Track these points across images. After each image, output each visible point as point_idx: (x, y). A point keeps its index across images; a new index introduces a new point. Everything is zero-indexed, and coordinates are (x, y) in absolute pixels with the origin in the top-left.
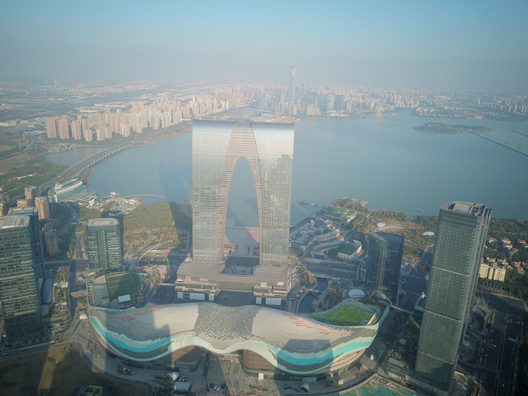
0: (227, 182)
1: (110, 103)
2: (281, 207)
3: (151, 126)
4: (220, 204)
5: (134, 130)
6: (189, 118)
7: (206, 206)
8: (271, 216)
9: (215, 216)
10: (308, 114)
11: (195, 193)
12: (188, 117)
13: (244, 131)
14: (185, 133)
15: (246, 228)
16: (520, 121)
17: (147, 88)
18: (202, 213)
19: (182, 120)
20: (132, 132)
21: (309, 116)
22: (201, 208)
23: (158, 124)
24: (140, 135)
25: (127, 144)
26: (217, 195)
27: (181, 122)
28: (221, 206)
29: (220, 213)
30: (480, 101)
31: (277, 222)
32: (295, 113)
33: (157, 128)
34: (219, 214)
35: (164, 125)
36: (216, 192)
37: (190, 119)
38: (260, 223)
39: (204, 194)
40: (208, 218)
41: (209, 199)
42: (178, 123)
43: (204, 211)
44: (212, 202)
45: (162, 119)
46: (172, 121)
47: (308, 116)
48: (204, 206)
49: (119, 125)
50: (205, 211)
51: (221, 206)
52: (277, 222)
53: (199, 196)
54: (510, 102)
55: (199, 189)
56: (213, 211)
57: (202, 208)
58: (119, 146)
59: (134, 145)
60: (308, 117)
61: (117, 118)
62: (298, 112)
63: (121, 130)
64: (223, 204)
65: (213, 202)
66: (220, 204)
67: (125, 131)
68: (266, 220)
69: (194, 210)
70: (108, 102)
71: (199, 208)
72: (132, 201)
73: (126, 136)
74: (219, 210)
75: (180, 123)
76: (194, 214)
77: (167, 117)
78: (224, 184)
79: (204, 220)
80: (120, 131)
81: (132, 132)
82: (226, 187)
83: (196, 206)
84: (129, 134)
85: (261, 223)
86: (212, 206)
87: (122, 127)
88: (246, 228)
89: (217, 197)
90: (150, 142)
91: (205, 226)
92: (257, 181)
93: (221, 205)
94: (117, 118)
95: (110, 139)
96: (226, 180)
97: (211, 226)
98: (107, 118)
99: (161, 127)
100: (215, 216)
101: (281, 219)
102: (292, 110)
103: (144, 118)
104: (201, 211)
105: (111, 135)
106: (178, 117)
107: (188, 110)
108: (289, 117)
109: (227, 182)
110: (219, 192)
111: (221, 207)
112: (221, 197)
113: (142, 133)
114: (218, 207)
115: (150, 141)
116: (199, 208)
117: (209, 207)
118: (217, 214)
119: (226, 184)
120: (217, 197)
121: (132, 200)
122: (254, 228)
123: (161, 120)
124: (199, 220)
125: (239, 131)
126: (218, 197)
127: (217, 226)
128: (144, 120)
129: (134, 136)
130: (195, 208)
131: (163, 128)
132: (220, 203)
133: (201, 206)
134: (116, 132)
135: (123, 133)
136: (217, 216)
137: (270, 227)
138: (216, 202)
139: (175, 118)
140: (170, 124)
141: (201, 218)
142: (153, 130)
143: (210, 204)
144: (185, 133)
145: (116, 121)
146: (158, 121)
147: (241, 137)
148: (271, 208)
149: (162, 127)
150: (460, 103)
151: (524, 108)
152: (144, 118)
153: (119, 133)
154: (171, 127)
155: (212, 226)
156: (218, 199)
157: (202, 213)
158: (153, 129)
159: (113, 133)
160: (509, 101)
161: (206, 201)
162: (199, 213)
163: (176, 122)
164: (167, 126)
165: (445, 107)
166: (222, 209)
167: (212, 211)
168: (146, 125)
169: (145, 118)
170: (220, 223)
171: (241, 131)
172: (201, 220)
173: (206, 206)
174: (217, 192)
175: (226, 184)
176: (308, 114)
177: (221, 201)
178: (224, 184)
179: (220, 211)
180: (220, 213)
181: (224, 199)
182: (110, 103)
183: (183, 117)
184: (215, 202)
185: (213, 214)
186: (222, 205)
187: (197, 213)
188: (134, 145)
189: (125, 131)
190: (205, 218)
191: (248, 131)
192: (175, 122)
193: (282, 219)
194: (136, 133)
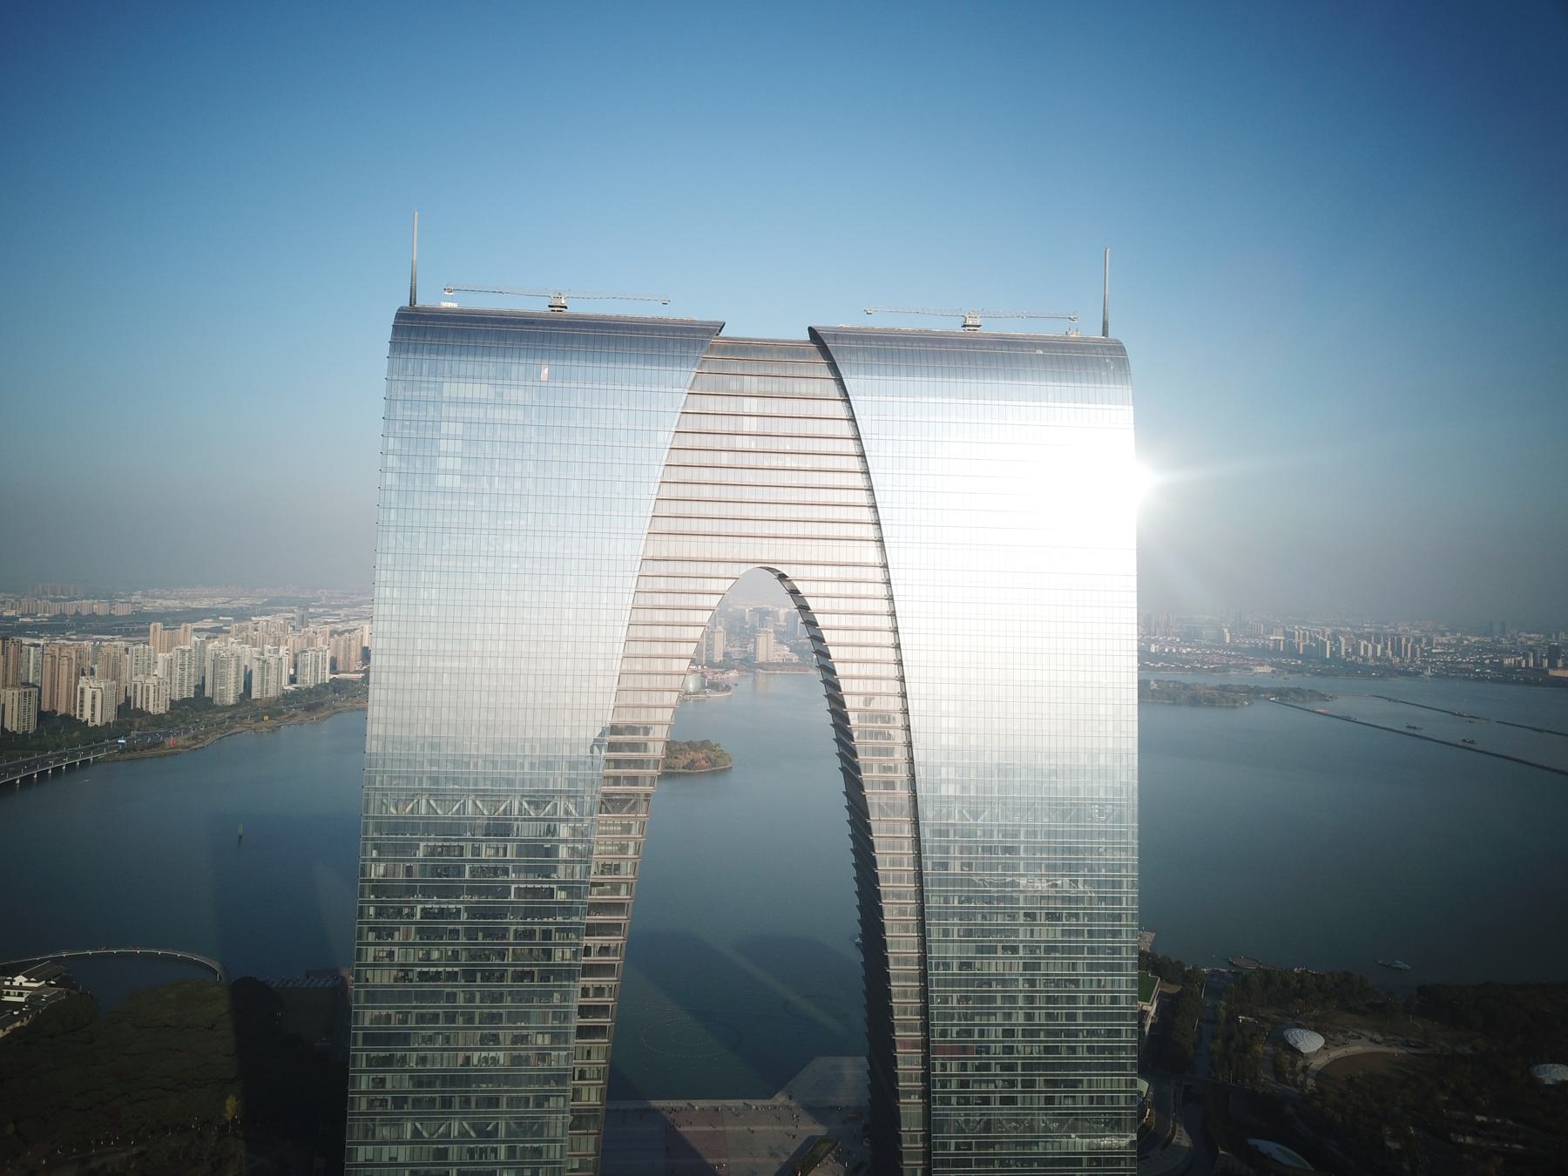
0: (639, 764)
1: (72, 637)
2: (1070, 950)
3: (208, 693)
4: (587, 951)
5: (138, 706)
6: (356, 672)
7: (470, 976)
8: (995, 1034)
9: (543, 1056)
10: (761, 658)
11: (377, 871)
12: (352, 670)
13: (772, 386)
14: (340, 712)
15: (656, 1104)
16: (1381, 677)
17: (220, 606)
18: (430, 1039)
19: (328, 677)
20: (127, 710)
21: (763, 663)
22: (421, 996)
23: (237, 682)
24: (158, 720)
25: (92, 748)
26: (561, 874)
27: (327, 682)
28: (589, 970)
29: (583, 1032)
30: (1228, 635)
31: (1040, 1086)
32: (718, 658)
33: (231, 699)
34: (574, 1042)
35: (262, 690)
36: (551, 852)
37: (361, 675)
38: (909, 1094)
39: (459, 871)
40: (483, 1079)
41: (499, 913)
42: (317, 686)
43: (451, 1018)
44: (517, 935)
45: (255, 667)
46: (293, 680)
47: (761, 666)
48: (452, 976)
49: (77, 683)
50: (460, 1022)
51: (589, 970)
52: (1040, 1086)
53: (411, 891)
54: (1308, 638)
55: (414, 828)
56: (526, 1017)
57: (435, 996)
58: (51, 756)
59: (122, 752)
60: (762, 668)
61: (70, 659)
62: (726, 654)
63: (82, 701)
64: (604, 950)
65: (530, 934)
66: (587, 951)
67: (93, 706)
68: (953, 1068)
69: (367, 1017)
70: (68, 634)
71: (404, 996)
72: (21, 987)
73: (98, 722)
74: (577, 1001)
75: (325, 685)
76: (361, 1055)
77: (272, 661)
78: (616, 780)
79: (447, 1103)
80: (75, 708)
81: (127, 710)
82: (633, 809)
83: (382, 978)
84: (111, 716)
85: (915, 1099)
86: (520, 976)
87: (87, 687)
88: (656, 1104)
89: (561, 896)
90: (194, 742)
91: (454, 1152)
92: (879, 751)
93: (594, 959)
94: (70, 659)
95: (25, 733)
96: (634, 747)
97: (502, 1156)
98: (36, 664)
99: (250, 696)
100: (543, 1056)
101: (1073, 1050)
102: (710, 648)
103: (182, 665)
104: (421, 1018)
105: (33, 721)
106: (317, 662)
107: (355, 654)
108: (700, 667)
109: (639, 764)
110: (584, 857)
111: (590, 982)
112: (595, 897)
113: (167, 713)
114: (570, 975)
115: (195, 737)
116: (404, 996)
117: (493, 987)
118: (558, 1036)
119: (634, 780)
120: (561, 896)
121: (20, 980)
122: (698, 1104)
123: (251, 672)
124: (399, 1102)
125: (734, 384)
126: (571, 888)
127: (554, 1152)
128: (183, 670)
129: (131, 724)
130: (372, 996)
131: (256, 699)
132: (587, 941)
133: (423, 976)
134: (62, 710)
135: (87, 715)
136: (558, 1059)
137: (987, 1127)
138: (556, 938)
139: (305, 666)
140: (286, 688)
141: (419, 1082)
142: (216, 706)
143: (502, 955)
144: (340, 712)
145: (64, 669)
146: (237, 674)
147: (750, 425)
148: (995, 966)
149: (253, 697)
150: (1178, 640)
151: (1366, 647)
152: (182, 665)
153: (73, 715)
154: (287, 698)
155: (511, 1152)
156: (567, 910)
157: (430, 1039)
158: (217, 700)
159: (42, 716)
160: (1305, 634)
161: (471, 933)
162: (405, 1039)
163: (308, 680)
164: (272, 693)
165: (1150, 647)
166: (599, 991)
167: (514, 1017)
168: (188, 691)
169: (190, 664)
170: (580, 1119)
171: (752, 384)
172: (416, 1102)
173: (470, 976)
174: (563, 853)
175: (634, 780)
176: (761, 658)
177: (592, 930)
178: (616, 780)
179: (584, 1011)
180: (583, 1032)
181: (618, 907)
182: (72, 637)
183: (334, 669)
184: (547, 935)
185: (523, 1039)
186: (605, 959)
187: (389, 1039)
188: (122, 752)
189: (93, 706)
190: (451, 1079)
191: (803, 387)
192: (303, 682)
193: (1082, 1053)
194: (141, 713)
